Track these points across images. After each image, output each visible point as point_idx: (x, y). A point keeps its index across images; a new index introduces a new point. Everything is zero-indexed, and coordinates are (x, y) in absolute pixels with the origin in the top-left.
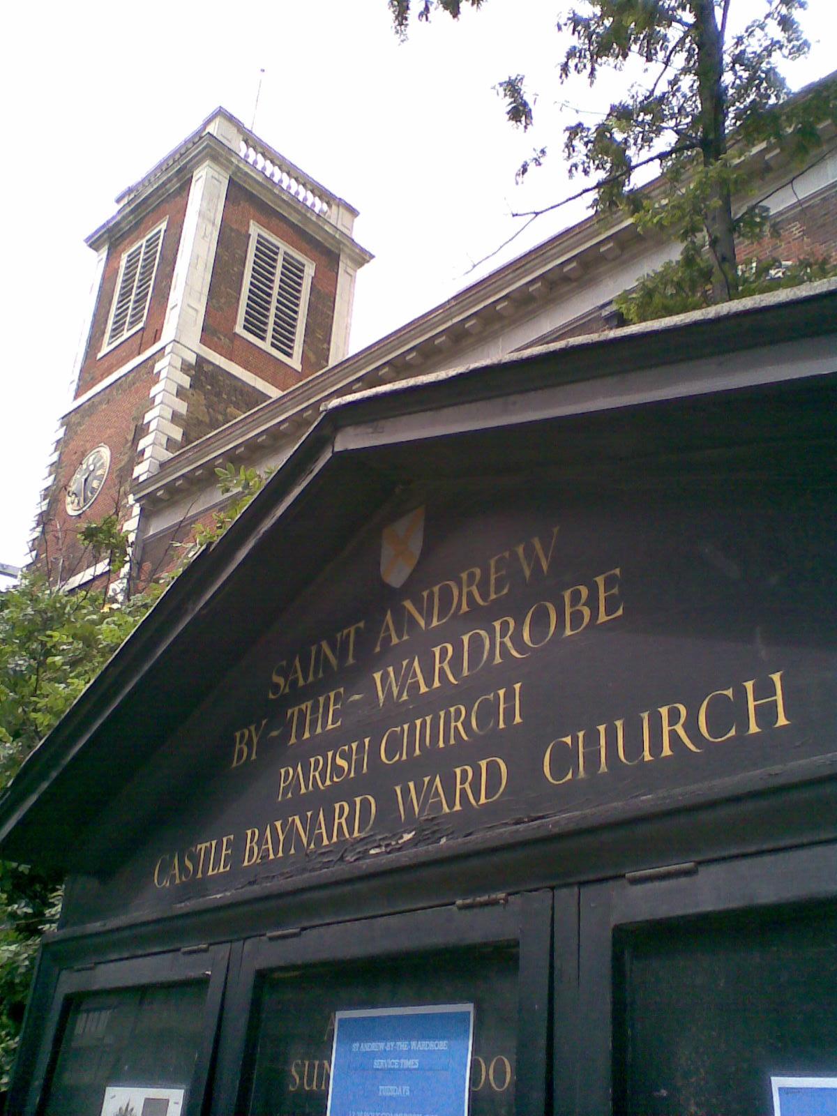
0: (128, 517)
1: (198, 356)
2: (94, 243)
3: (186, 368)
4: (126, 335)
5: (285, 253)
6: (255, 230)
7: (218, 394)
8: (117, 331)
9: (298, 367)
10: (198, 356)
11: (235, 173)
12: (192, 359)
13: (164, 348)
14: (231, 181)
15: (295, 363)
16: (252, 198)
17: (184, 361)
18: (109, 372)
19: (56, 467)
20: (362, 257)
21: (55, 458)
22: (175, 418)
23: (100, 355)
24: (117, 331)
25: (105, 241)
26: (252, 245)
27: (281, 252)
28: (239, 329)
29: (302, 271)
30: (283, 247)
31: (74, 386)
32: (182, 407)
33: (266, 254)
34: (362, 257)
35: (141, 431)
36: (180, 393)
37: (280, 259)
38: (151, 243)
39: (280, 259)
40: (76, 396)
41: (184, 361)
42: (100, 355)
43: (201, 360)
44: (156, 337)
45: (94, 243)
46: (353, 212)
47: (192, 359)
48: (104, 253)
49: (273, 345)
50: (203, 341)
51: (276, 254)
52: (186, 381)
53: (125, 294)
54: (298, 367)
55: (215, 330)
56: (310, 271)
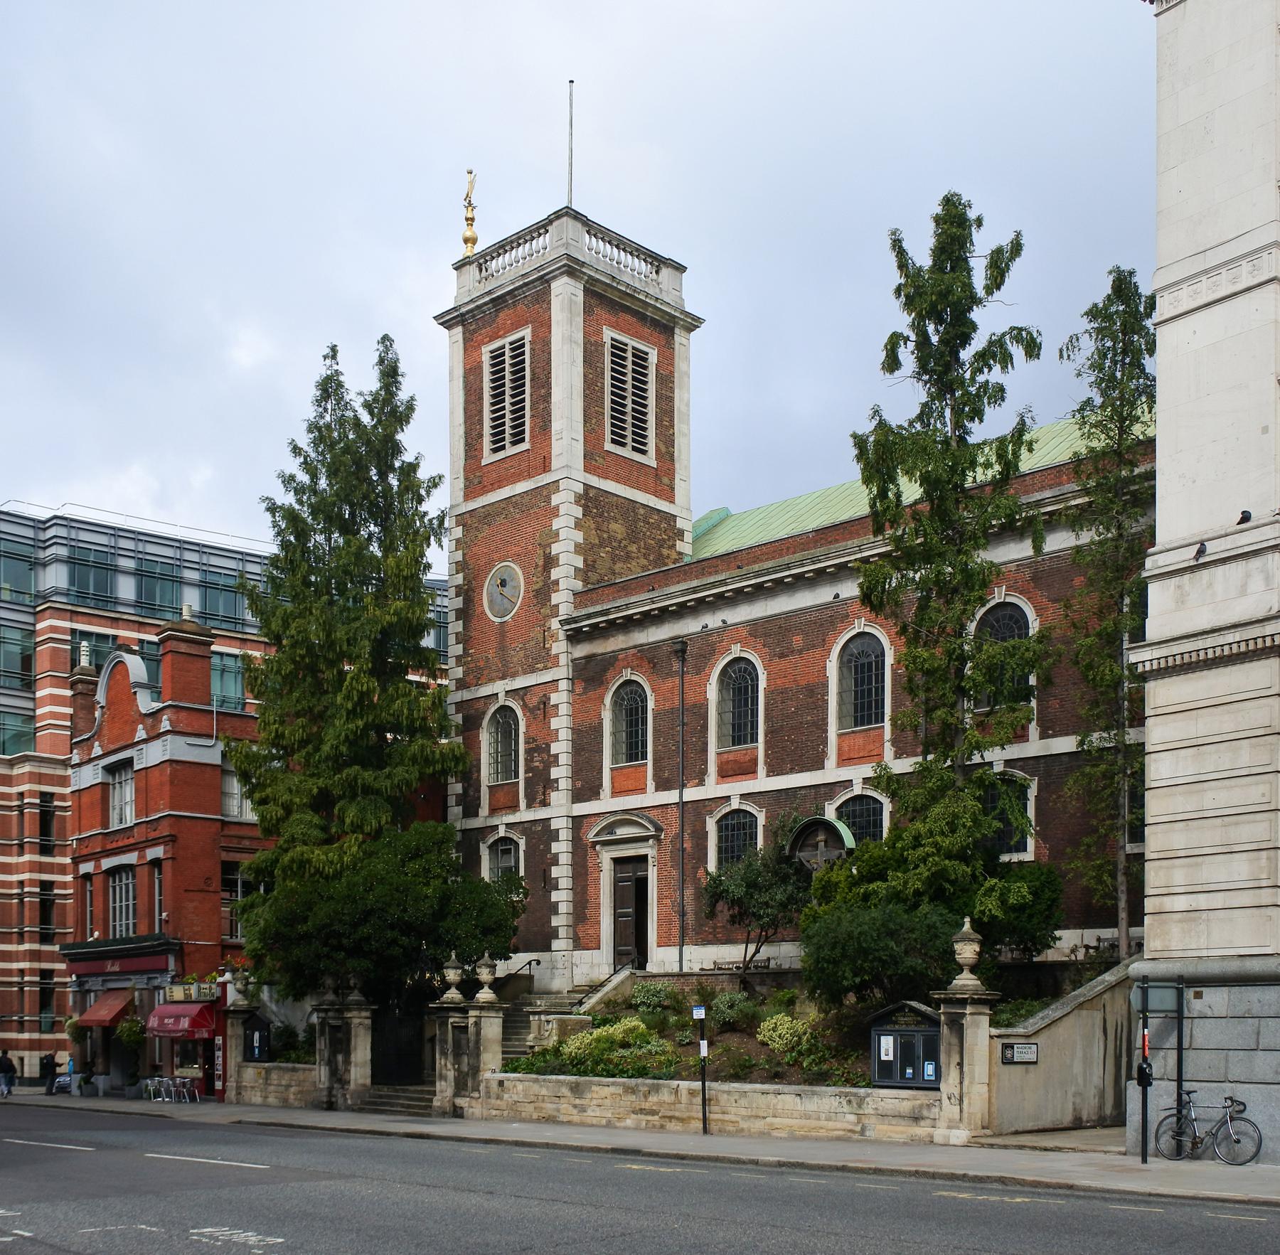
0: (554, 637)
5: (634, 348)
6: (608, 334)
7: (601, 515)
9: (654, 464)
11: (587, 282)
12: (580, 489)
14: (586, 290)
15: (650, 460)
16: (600, 297)
18: (499, 484)
20: (693, 323)
21: (459, 556)
22: (578, 549)
24: (498, 437)
26: (607, 350)
27: (630, 349)
28: (609, 446)
29: (645, 360)
30: (632, 343)
32: (579, 537)
33: (618, 348)
34: (693, 323)
35: (551, 562)
36: (578, 525)
37: (629, 355)
38: (518, 347)
39: (629, 355)
43: (587, 487)
45: (448, 320)
46: (681, 269)
48: (459, 329)
49: (634, 449)
50: (587, 469)
51: (625, 351)
52: (579, 512)
53: (498, 397)
54: (654, 464)
55: (593, 458)
56: (653, 357)
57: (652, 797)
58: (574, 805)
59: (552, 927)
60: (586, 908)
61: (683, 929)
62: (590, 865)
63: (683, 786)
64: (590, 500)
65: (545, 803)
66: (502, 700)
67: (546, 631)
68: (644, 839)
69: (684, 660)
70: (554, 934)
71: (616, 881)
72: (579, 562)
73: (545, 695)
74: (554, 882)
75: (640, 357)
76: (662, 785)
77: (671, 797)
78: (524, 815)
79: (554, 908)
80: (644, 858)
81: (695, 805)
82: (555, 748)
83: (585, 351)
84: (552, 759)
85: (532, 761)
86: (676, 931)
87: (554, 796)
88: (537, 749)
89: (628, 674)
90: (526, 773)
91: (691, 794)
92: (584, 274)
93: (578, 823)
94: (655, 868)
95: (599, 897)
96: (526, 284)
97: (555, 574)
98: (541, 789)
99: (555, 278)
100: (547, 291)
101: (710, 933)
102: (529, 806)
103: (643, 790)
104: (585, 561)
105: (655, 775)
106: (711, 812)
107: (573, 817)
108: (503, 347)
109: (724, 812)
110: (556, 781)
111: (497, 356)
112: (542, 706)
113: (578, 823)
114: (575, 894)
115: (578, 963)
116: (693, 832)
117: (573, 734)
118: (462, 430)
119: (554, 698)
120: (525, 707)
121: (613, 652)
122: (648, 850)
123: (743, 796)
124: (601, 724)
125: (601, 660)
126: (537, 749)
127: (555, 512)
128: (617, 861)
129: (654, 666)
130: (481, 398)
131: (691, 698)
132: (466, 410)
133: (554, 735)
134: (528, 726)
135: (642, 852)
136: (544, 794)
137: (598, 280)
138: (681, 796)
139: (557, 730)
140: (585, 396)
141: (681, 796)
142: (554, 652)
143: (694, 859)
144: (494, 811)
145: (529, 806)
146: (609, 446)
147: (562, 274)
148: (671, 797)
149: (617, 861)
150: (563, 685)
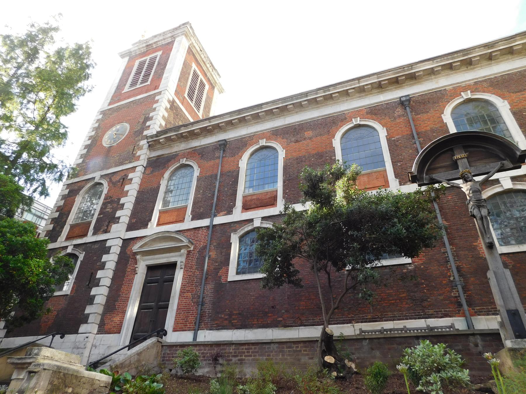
0: (141, 148)
1: (173, 99)
2: (123, 56)
3: (169, 101)
4: (138, 86)
7: (177, 115)
8: (144, 81)
10: (173, 99)
12: (171, 99)
13: (161, 91)
17: (168, 99)
18: (129, 97)
19: (96, 129)
23: (123, 92)
24: (134, 83)
25: (127, 55)
31: (109, 101)
32: (166, 115)
35: (148, 119)
36: (166, 109)
40: (109, 104)
41: (168, 99)
42: (123, 92)
43: (174, 101)
44: (156, 88)
45: (123, 56)
47: (171, 99)
48: (126, 59)
50: (175, 94)
52: (169, 106)
56: (207, 87)
57: (189, 224)
58: (128, 232)
59: (84, 314)
60: (116, 301)
61: (202, 316)
62: (128, 270)
63: (215, 216)
64: (173, 106)
65: (106, 231)
66: (96, 180)
67: (137, 147)
68: (177, 249)
69: (224, 151)
70: (85, 319)
71: (147, 282)
72: (164, 124)
73: (125, 175)
74: (96, 281)
75: (202, 85)
76: (196, 216)
77: (205, 222)
78: (90, 238)
79: (91, 300)
80: (173, 266)
81: (222, 227)
82: (122, 201)
83: (185, 61)
84: (119, 206)
85: (105, 208)
86: (191, 319)
87: (114, 227)
88: (112, 202)
89: (184, 161)
90: (99, 215)
91: (219, 220)
92: (191, 40)
93: (127, 242)
94: (182, 271)
95: (129, 292)
96: (164, 39)
97: (148, 124)
98: (106, 223)
99: (179, 36)
100: (172, 43)
101: (226, 319)
102: (94, 234)
103: (182, 221)
104: (166, 125)
105: (192, 211)
106: (235, 231)
107: (124, 240)
108: (147, 59)
109: (246, 229)
110: (119, 218)
111: (142, 64)
112: (122, 180)
113: (127, 242)
114: (110, 292)
115: (98, 344)
116: (219, 244)
117: (137, 194)
118: (116, 85)
119: (131, 176)
120: (110, 182)
121: (176, 152)
122: (179, 258)
123: (264, 219)
124: (158, 188)
125: (167, 157)
126: (112, 202)
127: (157, 101)
128: (151, 268)
129: (202, 156)
130: (129, 74)
131: (227, 168)
132: (120, 79)
133: (126, 194)
134: (109, 191)
135: (173, 260)
136: (107, 226)
137: (194, 47)
138: (212, 221)
139: (128, 191)
140: (181, 74)
141: (212, 221)
142: (138, 154)
143: (217, 262)
144: (68, 238)
145: (94, 234)
146: (186, 95)
147: (183, 34)
148: (205, 222)
149: (151, 268)
150: (140, 169)
